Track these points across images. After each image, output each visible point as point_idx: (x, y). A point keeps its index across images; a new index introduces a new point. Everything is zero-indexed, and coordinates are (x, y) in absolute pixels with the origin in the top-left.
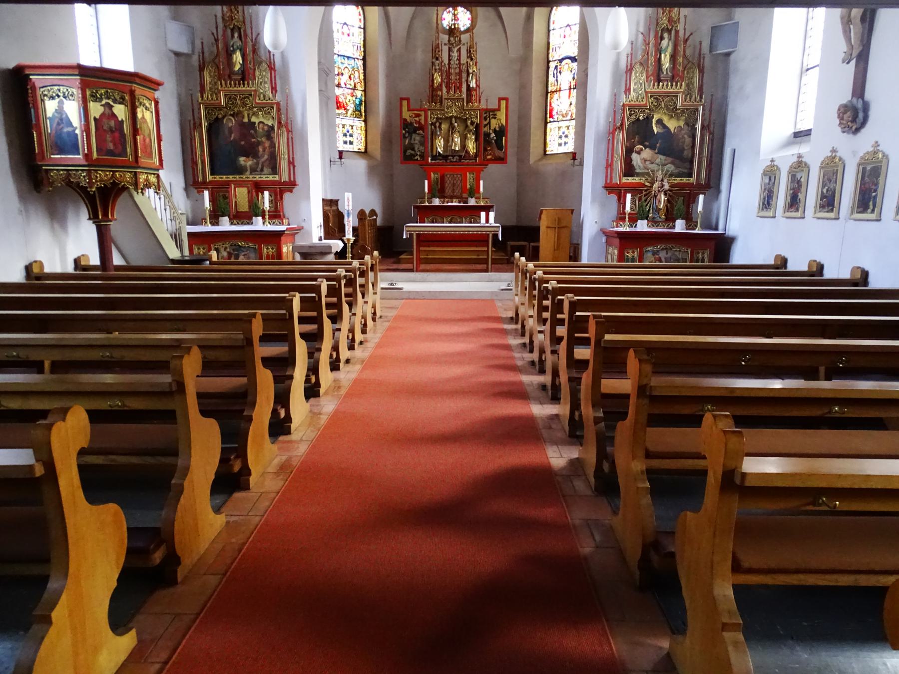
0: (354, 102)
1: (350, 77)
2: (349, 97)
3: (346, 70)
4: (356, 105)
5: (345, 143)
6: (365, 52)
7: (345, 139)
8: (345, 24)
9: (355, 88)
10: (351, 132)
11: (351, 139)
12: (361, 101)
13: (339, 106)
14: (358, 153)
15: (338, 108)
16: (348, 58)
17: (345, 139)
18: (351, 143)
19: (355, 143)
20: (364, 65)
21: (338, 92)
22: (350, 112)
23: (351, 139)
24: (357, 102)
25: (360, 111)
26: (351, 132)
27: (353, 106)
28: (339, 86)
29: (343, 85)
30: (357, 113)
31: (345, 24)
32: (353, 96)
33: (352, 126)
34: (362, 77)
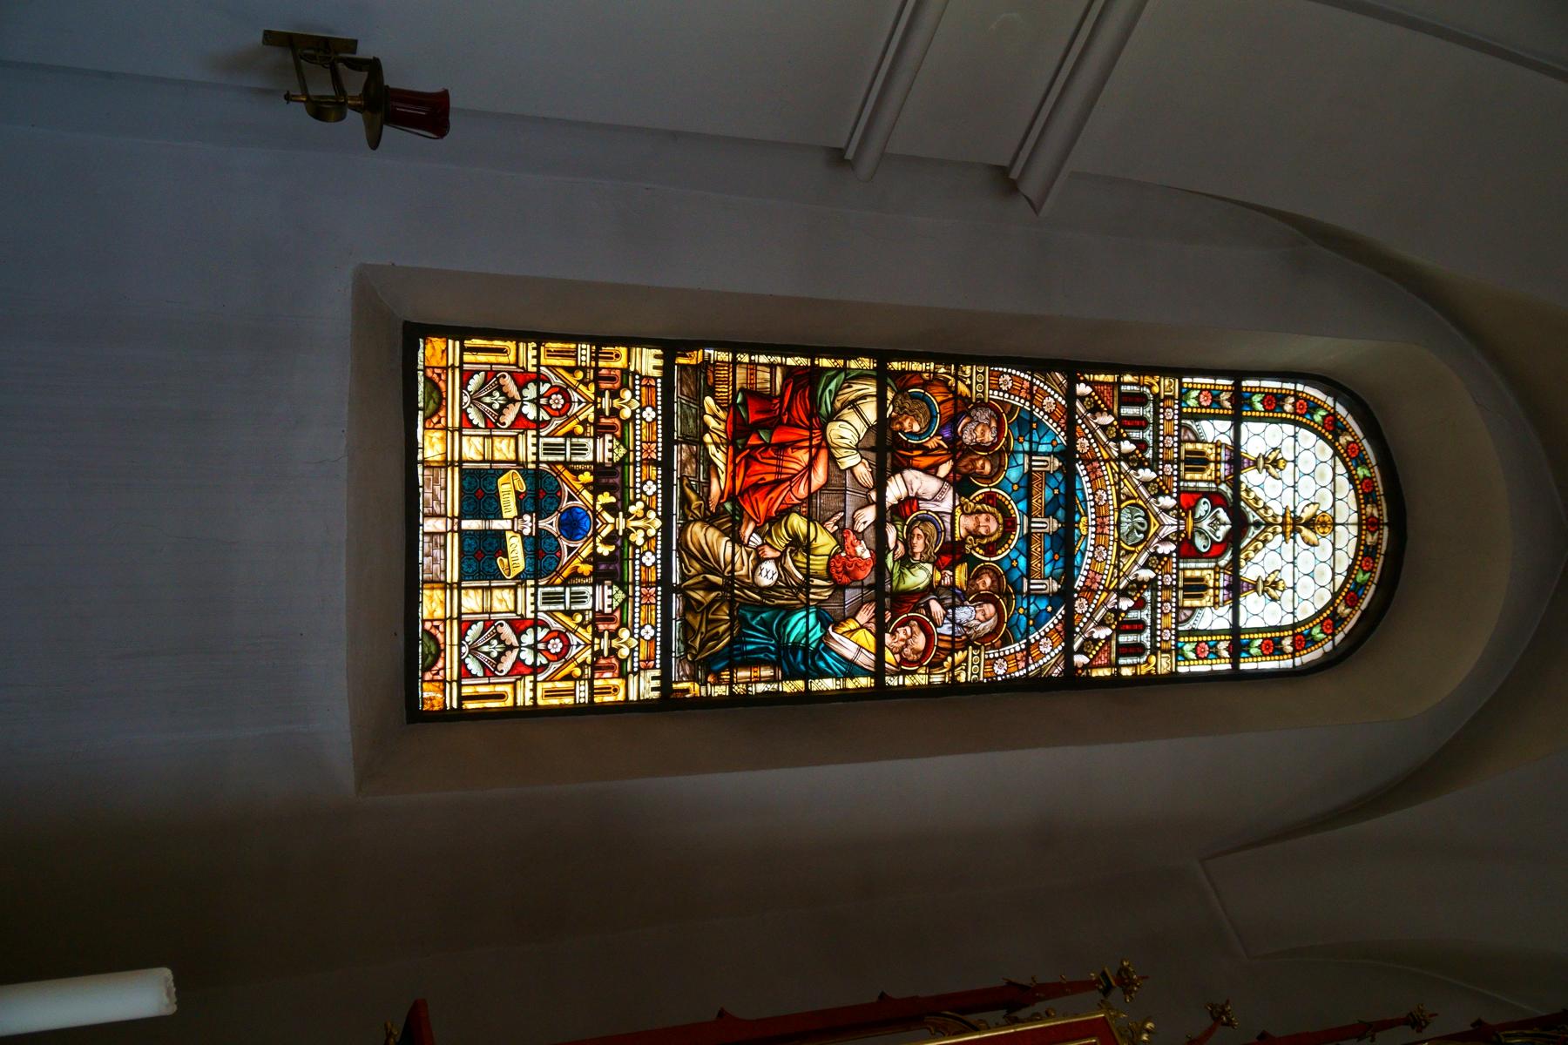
0: (796, 591)
1: (951, 553)
2: (825, 543)
3: (991, 526)
4: (775, 605)
5: (479, 490)
6: (1116, 681)
7: (509, 488)
8: (1240, 524)
9: (893, 605)
10: (578, 554)
11: (516, 557)
12: (806, 660)
13: (778, 421)
14: (412, 649)
15: (737, 435)
16: (1065, 543)
17: (509, 488)
18: (481, 557)
19: (472, 601)
20: (1038, 684)
21: (847, 432)
22: (724, 548)
23: (516, 557)
24: (799, 626)
25: (737, 658)
26: (578, 554)
27: (767, 575)
28: (888, 450)
29: (895, 491)
30: (725, 621)
31: (1240, 524)
32: (840, 574)
33: (608, 570)
34: (971, 667)
